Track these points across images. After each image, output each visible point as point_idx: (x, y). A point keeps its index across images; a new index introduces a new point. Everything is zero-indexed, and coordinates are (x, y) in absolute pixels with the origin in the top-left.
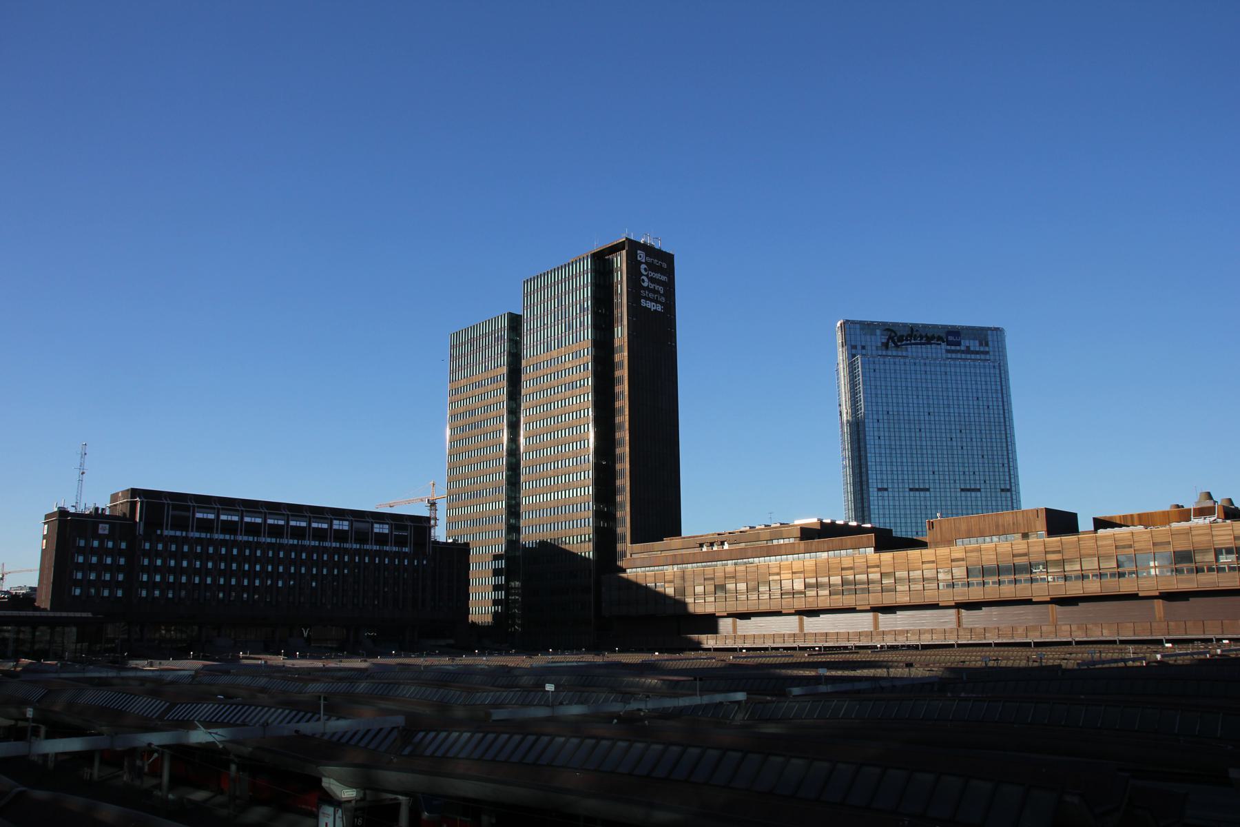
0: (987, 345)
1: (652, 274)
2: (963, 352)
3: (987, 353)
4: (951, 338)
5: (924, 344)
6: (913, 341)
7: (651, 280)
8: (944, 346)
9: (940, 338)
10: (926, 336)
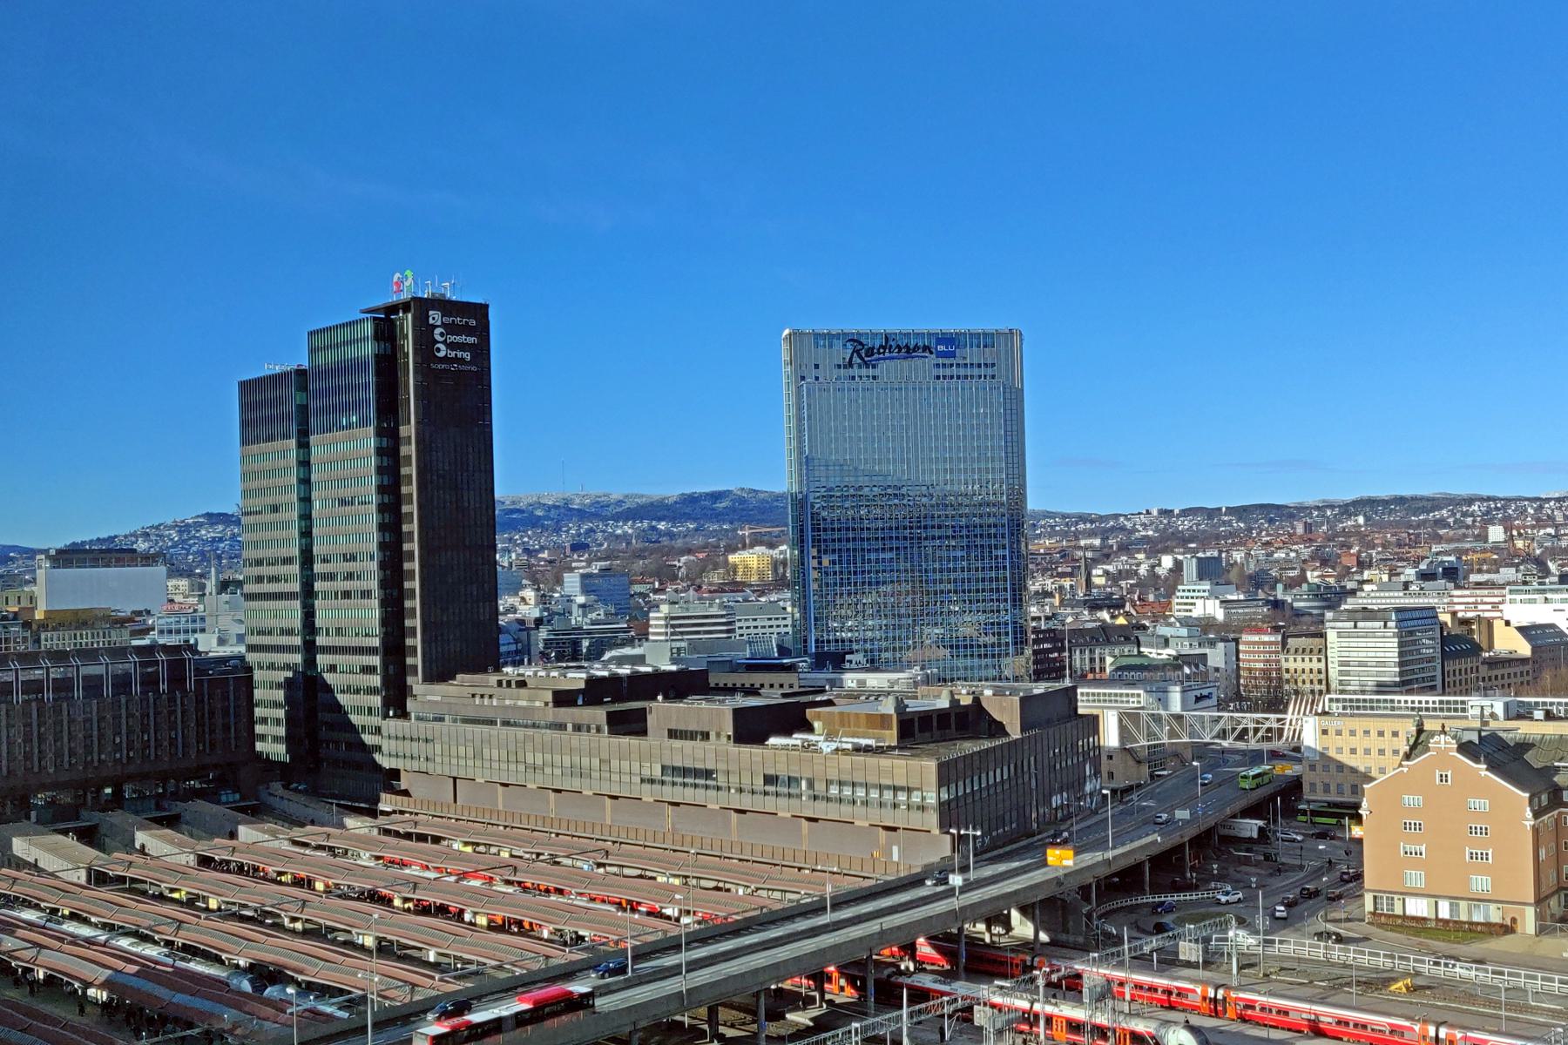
1: (451, 339)
4: (941, 348)
5: (905, 358)
6: (887, 355)
7: (451, 346)
8: (933, 359)
9: (926, 348)
10: (907, 346)
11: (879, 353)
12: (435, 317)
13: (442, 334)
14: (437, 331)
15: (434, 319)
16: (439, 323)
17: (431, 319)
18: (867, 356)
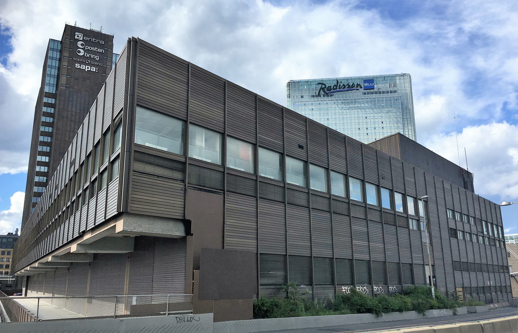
0: (395, 86)
2: (376, 93)
3: (395, 92)
6: (338, 90)
8: (362, 90)
11: (334, 89)
12: (79, 36)
13: (82, 45)
14: (80, 43)
15: (78, 36)
16: (81, 39)
18: (328, 91)
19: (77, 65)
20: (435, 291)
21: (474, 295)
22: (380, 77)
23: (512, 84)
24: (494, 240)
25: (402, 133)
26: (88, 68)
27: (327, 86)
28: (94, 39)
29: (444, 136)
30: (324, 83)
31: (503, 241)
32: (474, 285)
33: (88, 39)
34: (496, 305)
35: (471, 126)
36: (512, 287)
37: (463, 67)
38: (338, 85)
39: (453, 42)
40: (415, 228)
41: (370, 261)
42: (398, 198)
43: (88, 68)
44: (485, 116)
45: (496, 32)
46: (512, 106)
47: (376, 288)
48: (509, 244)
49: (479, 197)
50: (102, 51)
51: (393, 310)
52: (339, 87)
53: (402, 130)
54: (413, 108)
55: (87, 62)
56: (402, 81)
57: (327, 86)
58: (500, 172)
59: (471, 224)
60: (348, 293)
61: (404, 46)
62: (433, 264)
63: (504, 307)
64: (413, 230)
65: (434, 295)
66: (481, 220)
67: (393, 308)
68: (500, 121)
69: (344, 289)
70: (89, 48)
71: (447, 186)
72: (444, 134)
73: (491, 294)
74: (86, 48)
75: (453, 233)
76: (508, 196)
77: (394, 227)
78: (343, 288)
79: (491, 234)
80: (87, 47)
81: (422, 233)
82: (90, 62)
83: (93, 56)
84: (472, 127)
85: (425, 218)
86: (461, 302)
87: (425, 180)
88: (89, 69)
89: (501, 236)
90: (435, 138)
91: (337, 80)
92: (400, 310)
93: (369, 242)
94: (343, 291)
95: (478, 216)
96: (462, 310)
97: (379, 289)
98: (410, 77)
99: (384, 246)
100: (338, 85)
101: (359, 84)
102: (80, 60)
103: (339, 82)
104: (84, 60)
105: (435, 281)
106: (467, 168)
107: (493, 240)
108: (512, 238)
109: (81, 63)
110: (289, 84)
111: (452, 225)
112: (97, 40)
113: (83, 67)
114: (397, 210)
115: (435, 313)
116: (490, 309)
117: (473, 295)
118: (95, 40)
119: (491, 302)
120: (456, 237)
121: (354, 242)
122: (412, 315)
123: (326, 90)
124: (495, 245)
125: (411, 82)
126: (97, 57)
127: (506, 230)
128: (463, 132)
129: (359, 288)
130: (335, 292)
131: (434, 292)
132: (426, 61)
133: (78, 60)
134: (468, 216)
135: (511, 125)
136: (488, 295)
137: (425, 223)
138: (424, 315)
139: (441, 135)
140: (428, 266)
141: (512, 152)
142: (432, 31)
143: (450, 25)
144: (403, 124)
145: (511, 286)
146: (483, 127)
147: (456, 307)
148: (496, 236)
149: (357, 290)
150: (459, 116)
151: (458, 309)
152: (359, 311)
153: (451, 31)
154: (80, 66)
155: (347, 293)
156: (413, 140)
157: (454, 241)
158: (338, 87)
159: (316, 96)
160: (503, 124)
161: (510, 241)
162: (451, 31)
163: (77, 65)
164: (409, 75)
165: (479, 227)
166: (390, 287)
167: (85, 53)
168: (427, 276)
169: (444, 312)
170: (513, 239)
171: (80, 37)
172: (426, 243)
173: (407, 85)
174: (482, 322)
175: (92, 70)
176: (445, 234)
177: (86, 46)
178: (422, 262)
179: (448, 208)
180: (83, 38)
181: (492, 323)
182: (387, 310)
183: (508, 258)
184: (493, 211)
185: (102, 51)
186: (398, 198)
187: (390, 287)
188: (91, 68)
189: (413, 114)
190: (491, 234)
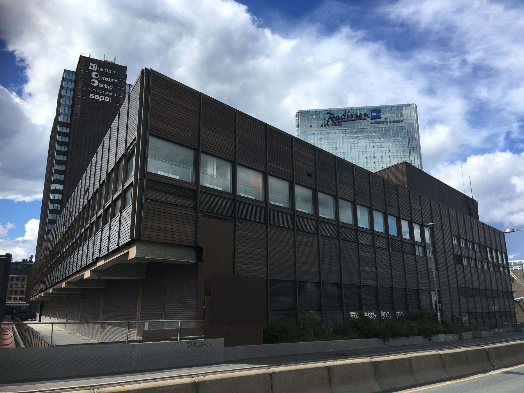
0: (401, 115)
2: (383, 122)
3: (402, 121)
6: (346, 119)
8: (369, 120)
11: (342, 119)
12: (93, 67)
13: (96, 75)
14: (93, 74)
15: (92, 67)
16: (95, 70)
17: (90, 67)
18: (336, 120)
19: (91, 96)
20: (441, 316)
21: (480, 320)
22: (387, 107)
23: (514, 114)
24: (499, 265)
25: (408, 162)
26: (102, 98)
27: (335, 116)
28: (107, 70)
29: (449, 164)
30: (333, 113)
31: (507, 267)
32: (479, 310)
33: (102, 70)
34: (501, 330)
35: (475, 155)
36: (516, 312)
37: (466, 97)
38: (346, 115)
39: (457, 74)
40: (421, 255)
41: (377, 287)
42: (405, 226)
43: (102, 98)
44: (489, 146)
45: (499, 63)
46: (515, 135)
47: (383, 313)
48: (513, 270)
49: (483, 224)
50: (116, 81)
51: (400, 335)
52: (347, 117)
53: (408, 159)
54: (419, 138)
55: (101, 92)
56: (408, 111)
57: (335, 116)
58: (503, 200)
59: (476, 250)
60: (356, 318)
61: (409, 77)
62: (439, 290)
63: (508, 332)
64: (419, 256)
65: (440, 320)
66: (486, 247)
67: (401, 333)
68: (503, 150)
69: (353, 314)
70: (103, 78)
71: (452, 213)
72: (449, 162)
73: (496, 319)
74: (100, 79)
75: (458, 259)
76: (512, 224)
77: (401, 254)
78: (351, 314)
79: (495, 261)
80: (101, 78)
81: (429, 260)
82: (104, 92)
83: (107, 86)
84: (476, 156)
85: (431, 244)
86: (466, 327)
87: (431, 207)
88: (103, 99)
89: (505, 262)
90: (440, 166)
91: (345, 110)
92: (407, 335)
93: (376, 268)
94: (351, 316)
95: (483, 242)
96: (467, 335)
97: (386, 315)
98: (416, 107)
99: (391, 272)
100: (346, 115)
101: (367, 114)
102: (94, 90)
103: (347, 112)
104: (98, 90)
105: (441, 306)
106: (472, 196)
107: (497, 266)
108: (515, 264)
109: (95, 93)
110: (298, 114)
111: (457, 252)
112: (111, 71)
113: (97, 97)
114: (404, 237)
115: (441, 337)
116: (495, 334)
117: (478, 320)
118: (108, 71)
119: (496, 327)
120: (462, 263)
121: (362, 268)
122: (419, 339)
123: (334, 120)
124: (499, 271)
125: (417, 112)
126: (111, 88)
127: (510, 257)
128: (468, 161)
129: (367, 313)
130: (343, 317)
131: (440, 318)
132: (431, 92)
133: (93, 90)
134: (473, 243)
135: (514, 154)
136: (493, 320)
137: (431, 250)
138: (430, 340)
139: (446, 164)
140: (434, 292)
141: (515, 180)
142: (437, 62)
143: (454, 56)
144: (409, 153)
145: (515, 312)
146: (486, 156)
147: (461, 332)
148: (500, 262)
149: (365, 315)
150: (463, 145)
151: (464, 334)
152: (367, 336)
153: (455, 63)
154: (94, 96)
155: (355, 318)
156: (420, 168)
157: (459, 267)
158: (346, 117)
159: (325, 126)
160: (506, 153)
161: (514, 267)
162: (455, 63)
163: (91, 96)
164: (415, 105)
165: (484, 254)
166: (397, 313)
167: (99, 84)
168: (433, 302)
169: (450, 337)
170: (517, 265)
171: (94, 67)
172: (432, 269)
173: (414, 115)
174: (487, 347)
175: (105, 100)
176: (451, 261)
177: (100, 77)
178: (427, 288)
179: (453, 235)
180: (97, 69)
181: (497, 348)
182: (395, 335)
183: (513, 284)
184: (498, 239)
185: (116, 81)
186: (405, 226)
187: (397, 313)
188: (105, 98)
189: (419, 143)
190: (495, 261)
